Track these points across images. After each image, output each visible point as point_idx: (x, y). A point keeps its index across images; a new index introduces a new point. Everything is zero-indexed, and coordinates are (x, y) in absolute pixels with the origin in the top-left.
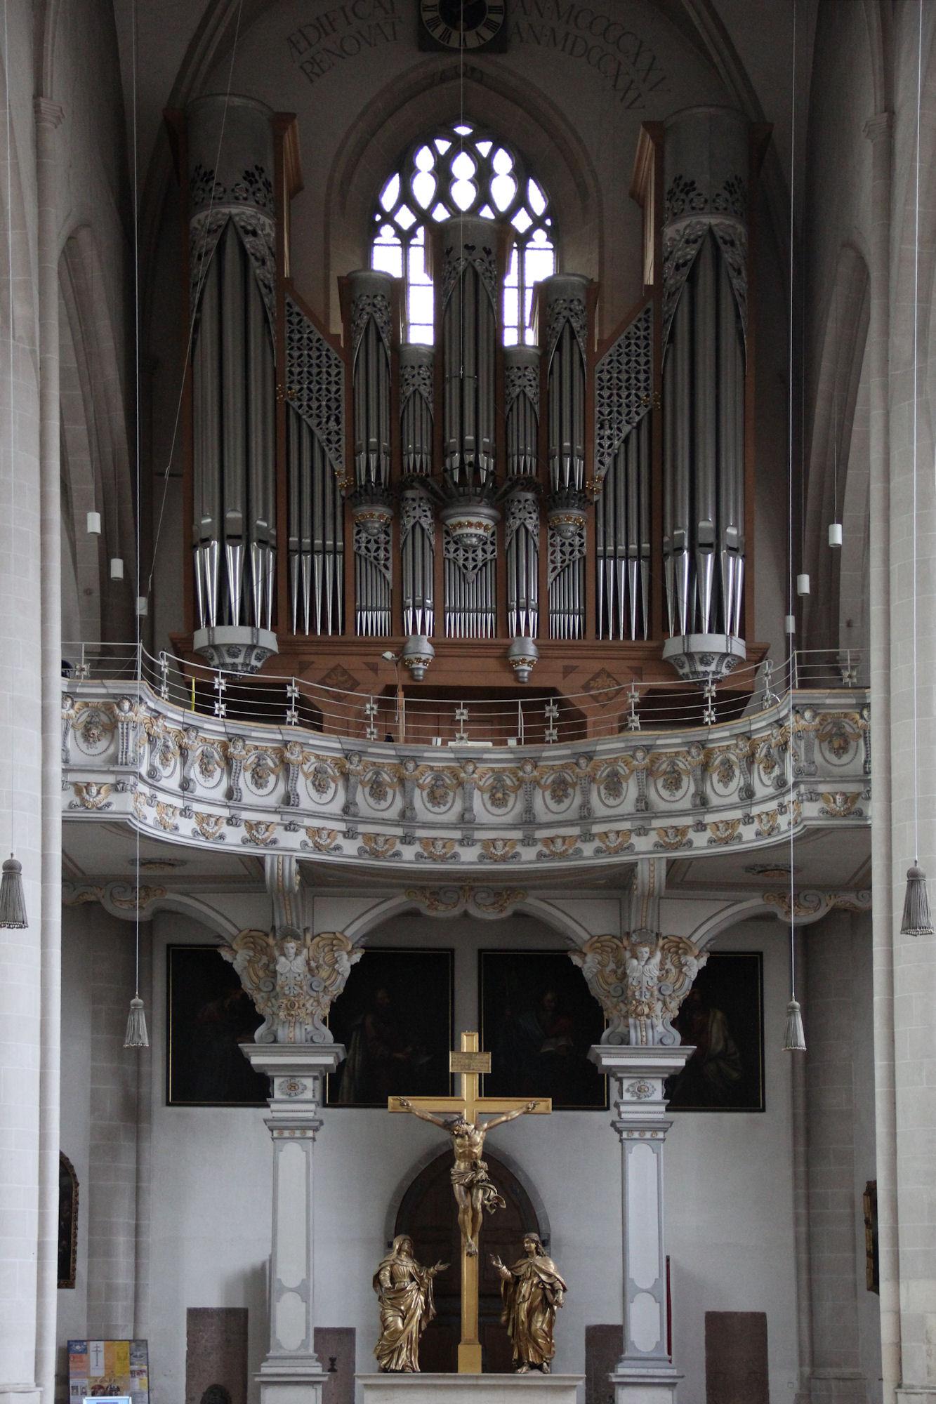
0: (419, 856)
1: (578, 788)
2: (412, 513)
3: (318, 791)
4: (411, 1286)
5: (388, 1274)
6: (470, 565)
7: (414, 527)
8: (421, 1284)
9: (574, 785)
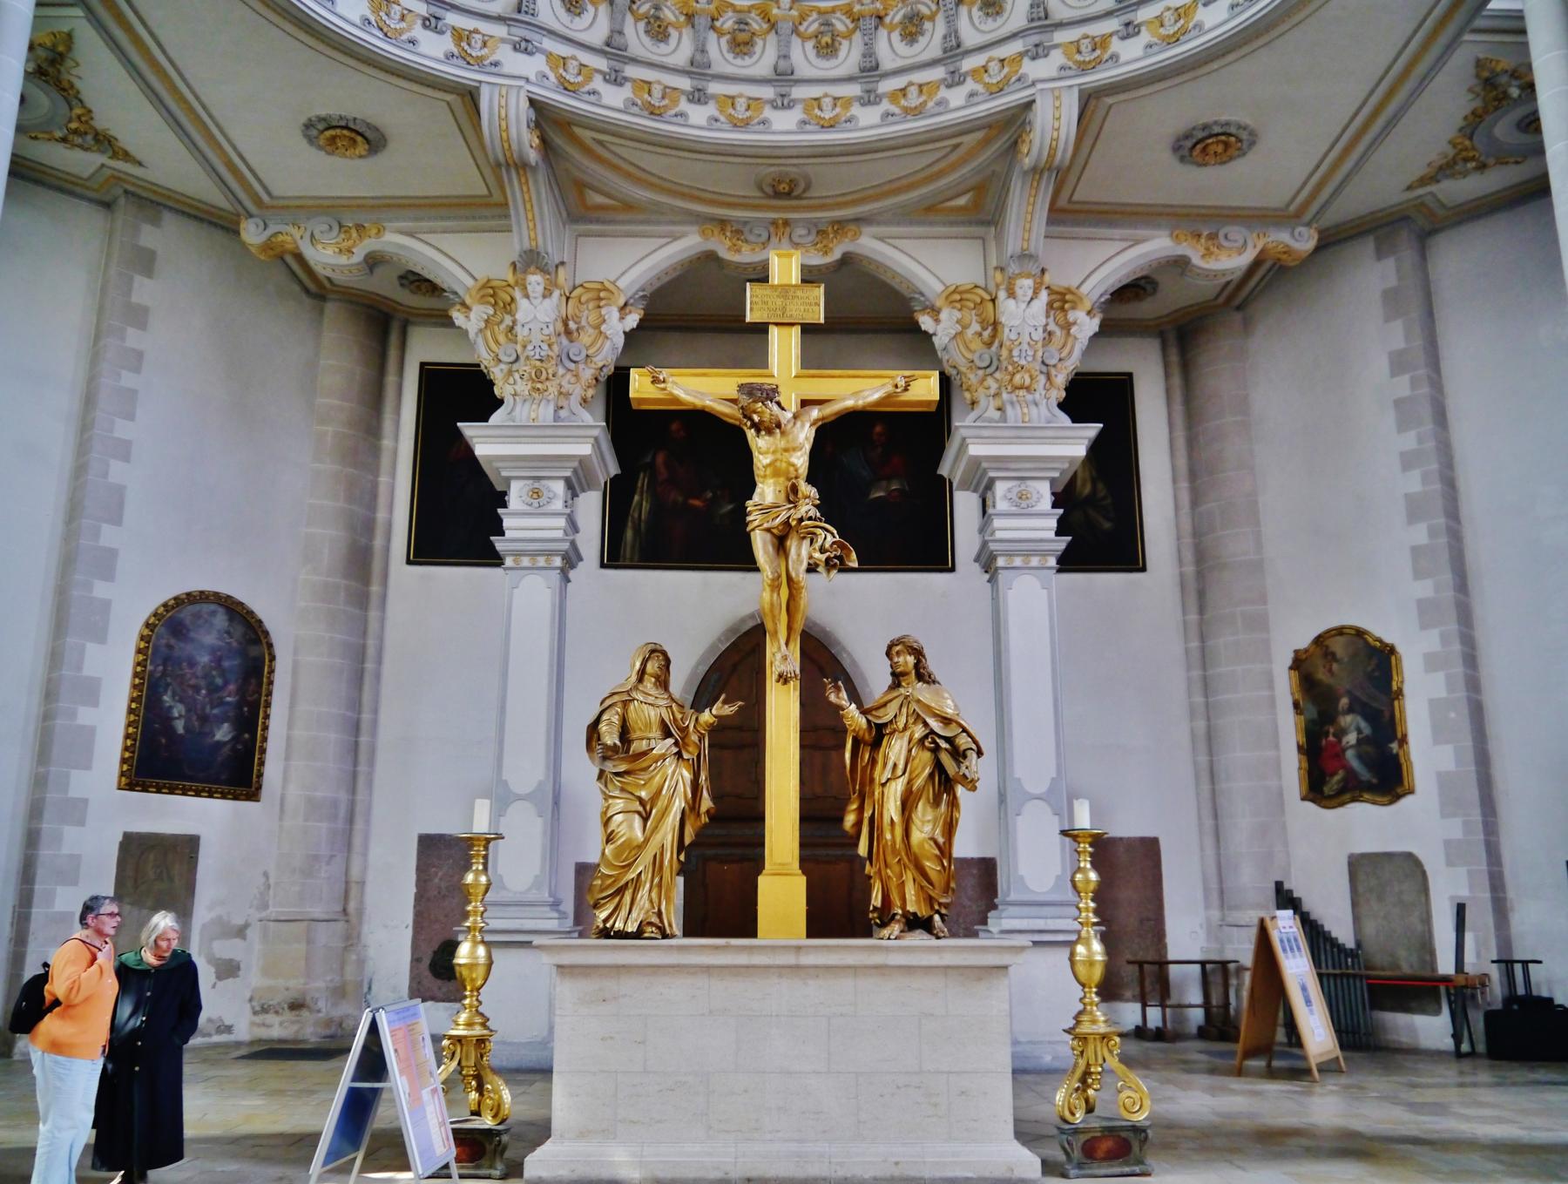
1: (940, 19)
3: (569, 10)
4: (664, 746)
5: (616, 719)
8: (685, 745)
9: (932, 18)
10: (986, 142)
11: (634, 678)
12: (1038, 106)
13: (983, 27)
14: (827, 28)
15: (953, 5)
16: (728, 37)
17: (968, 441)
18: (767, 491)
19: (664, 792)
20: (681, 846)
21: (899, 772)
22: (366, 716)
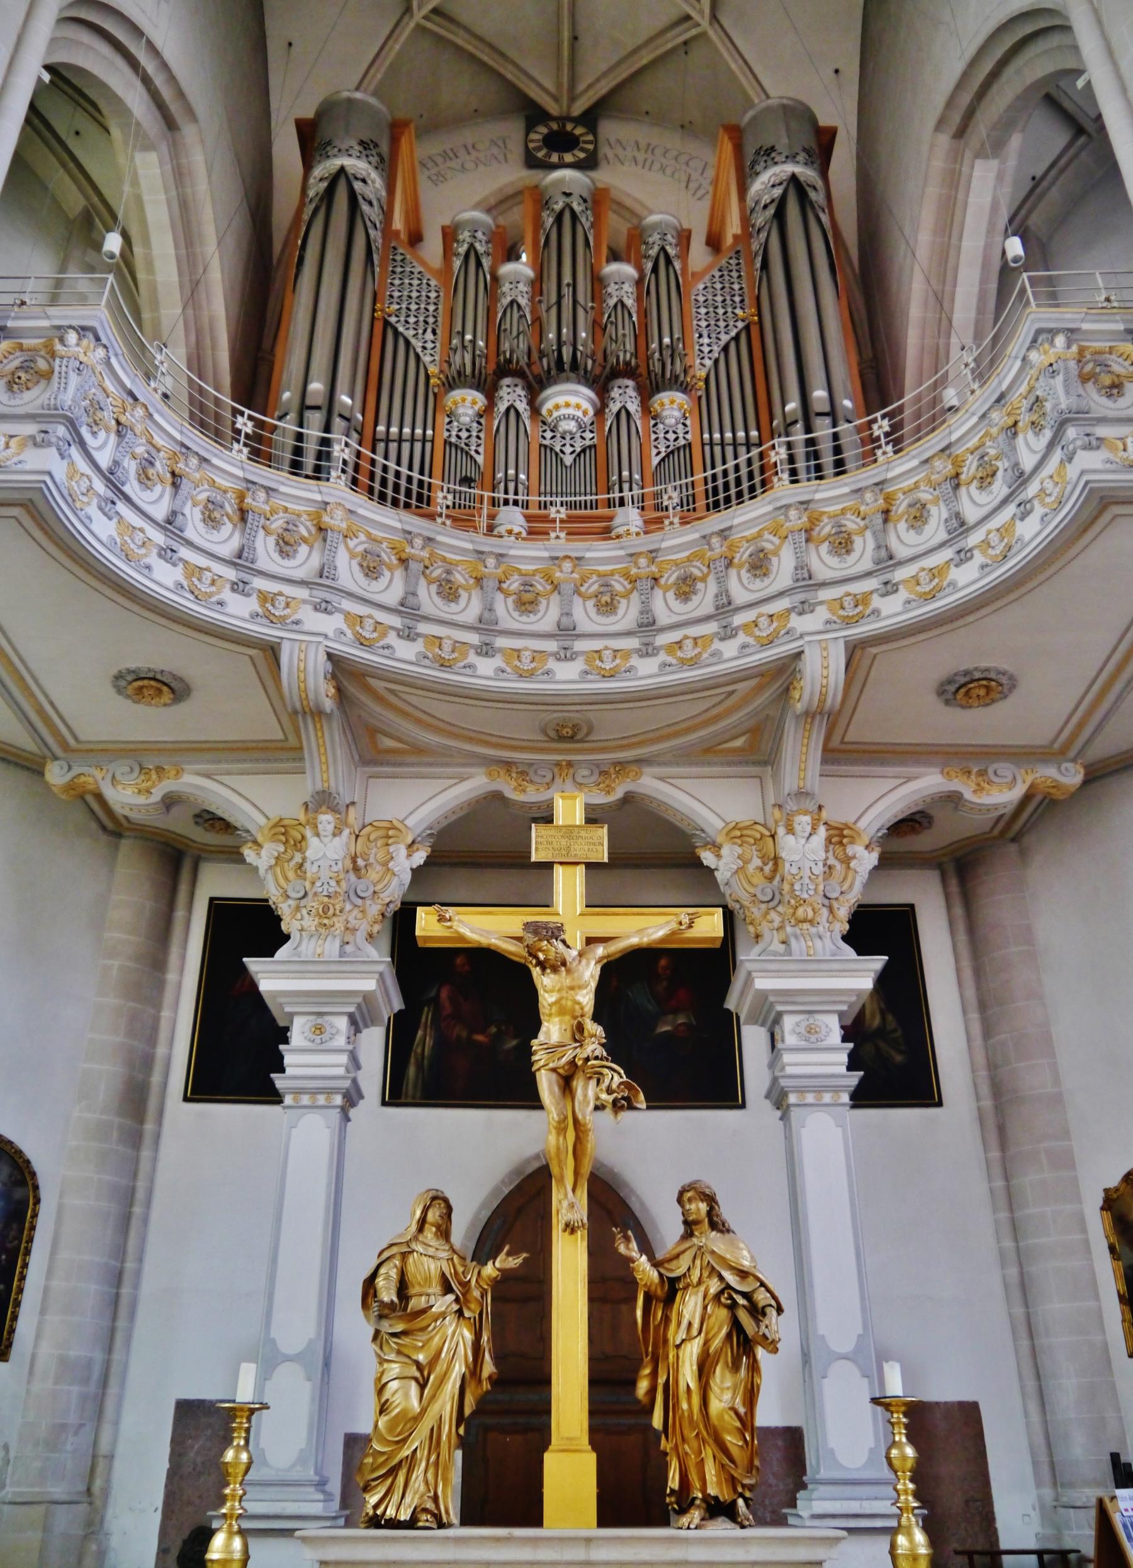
1: (711, 580)
2: (506, 397)
3: (367, 575)
4: (444, 1303)
5: (394, 1274)
6: (568, 449)
7: (508, 410)
8: (467, 1301)
9: (704, 579)
10: (759, 689)
11: (414, 1227)
12: (807, 656)
13: (751, 587)
14: (606, 589)
15: (723, 568)
16: (514, 597)
17: (754, 974)
18: (552, 1030)
19: (443, 1355)
20: (460, 1418)
21: (695, 1332)
22: (130, 1265)
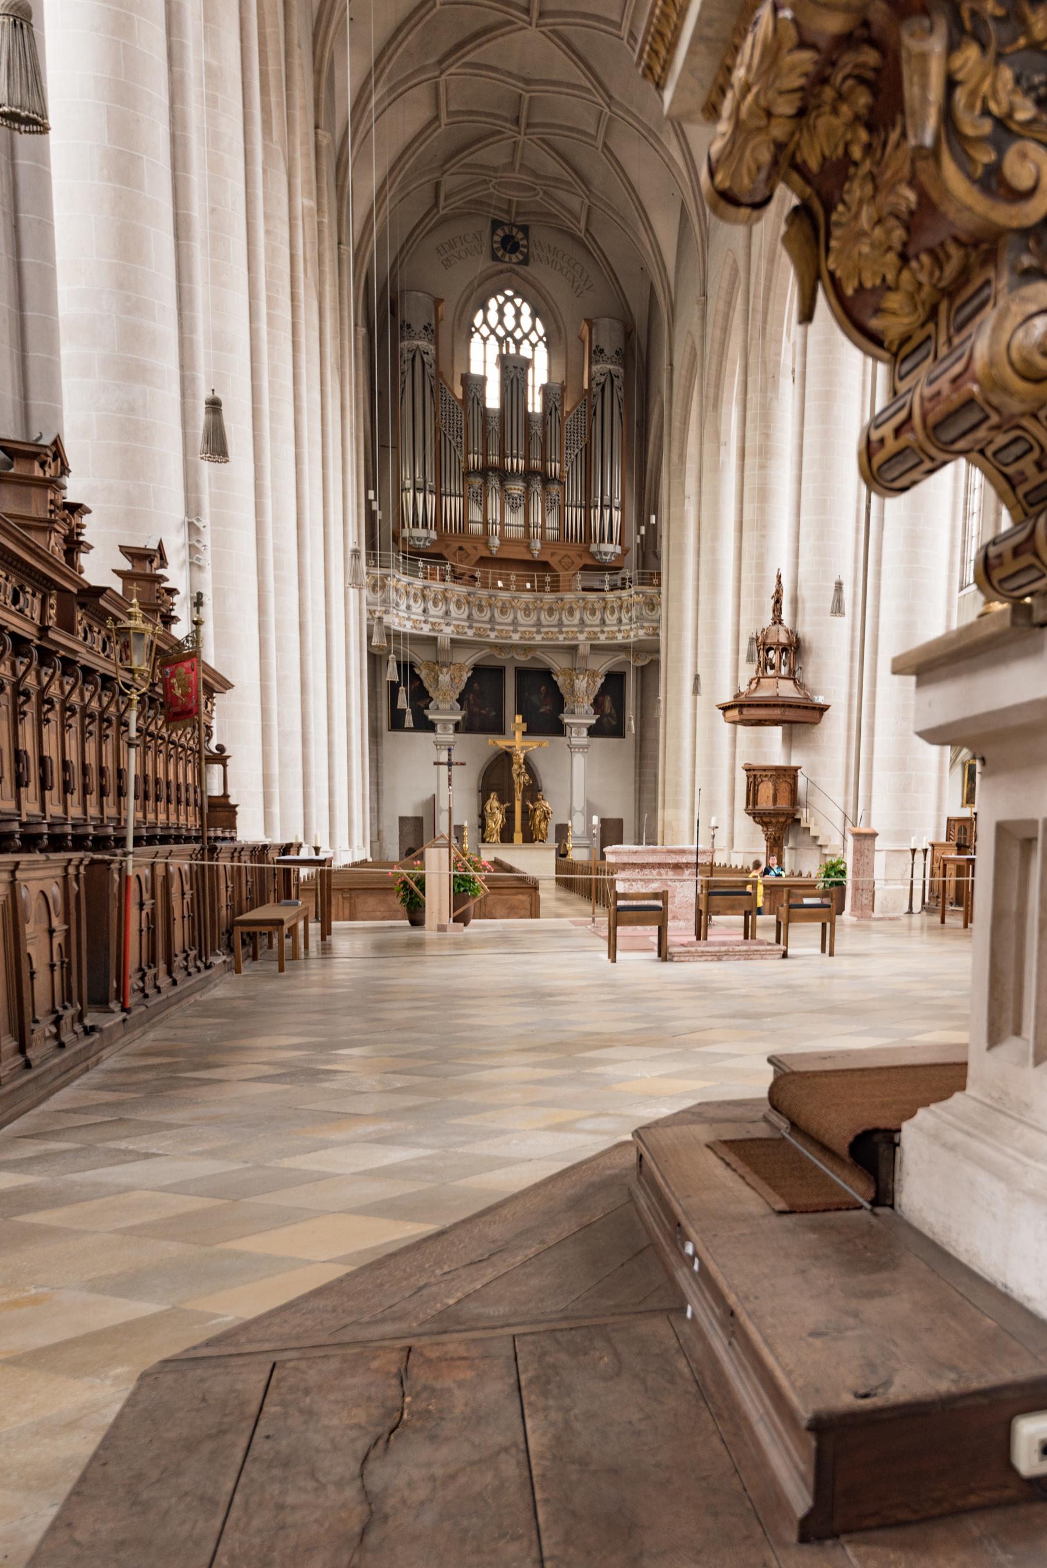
0: (497, 637)
4: (497, 812)
18: (515, 767)
